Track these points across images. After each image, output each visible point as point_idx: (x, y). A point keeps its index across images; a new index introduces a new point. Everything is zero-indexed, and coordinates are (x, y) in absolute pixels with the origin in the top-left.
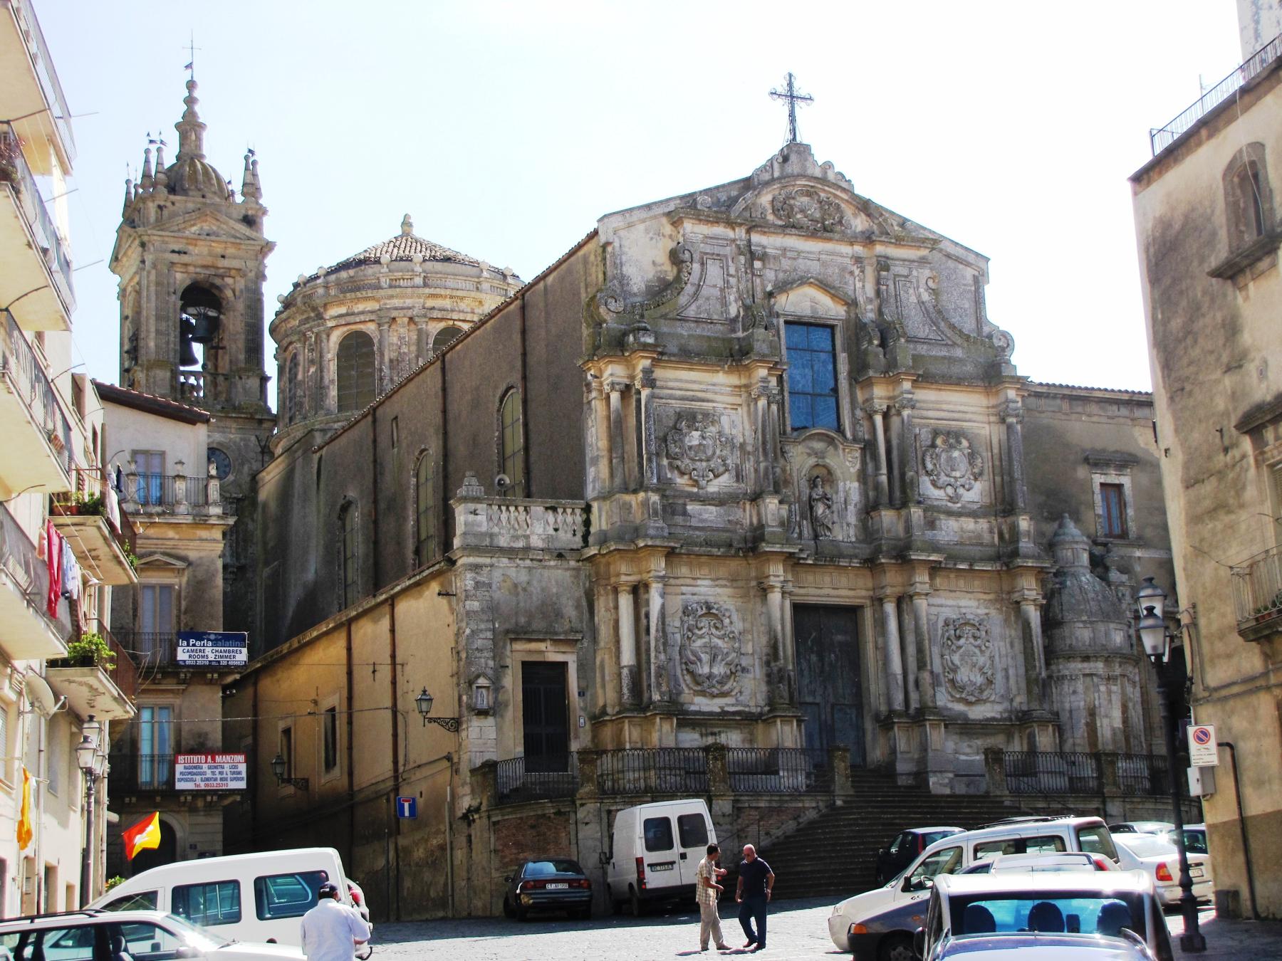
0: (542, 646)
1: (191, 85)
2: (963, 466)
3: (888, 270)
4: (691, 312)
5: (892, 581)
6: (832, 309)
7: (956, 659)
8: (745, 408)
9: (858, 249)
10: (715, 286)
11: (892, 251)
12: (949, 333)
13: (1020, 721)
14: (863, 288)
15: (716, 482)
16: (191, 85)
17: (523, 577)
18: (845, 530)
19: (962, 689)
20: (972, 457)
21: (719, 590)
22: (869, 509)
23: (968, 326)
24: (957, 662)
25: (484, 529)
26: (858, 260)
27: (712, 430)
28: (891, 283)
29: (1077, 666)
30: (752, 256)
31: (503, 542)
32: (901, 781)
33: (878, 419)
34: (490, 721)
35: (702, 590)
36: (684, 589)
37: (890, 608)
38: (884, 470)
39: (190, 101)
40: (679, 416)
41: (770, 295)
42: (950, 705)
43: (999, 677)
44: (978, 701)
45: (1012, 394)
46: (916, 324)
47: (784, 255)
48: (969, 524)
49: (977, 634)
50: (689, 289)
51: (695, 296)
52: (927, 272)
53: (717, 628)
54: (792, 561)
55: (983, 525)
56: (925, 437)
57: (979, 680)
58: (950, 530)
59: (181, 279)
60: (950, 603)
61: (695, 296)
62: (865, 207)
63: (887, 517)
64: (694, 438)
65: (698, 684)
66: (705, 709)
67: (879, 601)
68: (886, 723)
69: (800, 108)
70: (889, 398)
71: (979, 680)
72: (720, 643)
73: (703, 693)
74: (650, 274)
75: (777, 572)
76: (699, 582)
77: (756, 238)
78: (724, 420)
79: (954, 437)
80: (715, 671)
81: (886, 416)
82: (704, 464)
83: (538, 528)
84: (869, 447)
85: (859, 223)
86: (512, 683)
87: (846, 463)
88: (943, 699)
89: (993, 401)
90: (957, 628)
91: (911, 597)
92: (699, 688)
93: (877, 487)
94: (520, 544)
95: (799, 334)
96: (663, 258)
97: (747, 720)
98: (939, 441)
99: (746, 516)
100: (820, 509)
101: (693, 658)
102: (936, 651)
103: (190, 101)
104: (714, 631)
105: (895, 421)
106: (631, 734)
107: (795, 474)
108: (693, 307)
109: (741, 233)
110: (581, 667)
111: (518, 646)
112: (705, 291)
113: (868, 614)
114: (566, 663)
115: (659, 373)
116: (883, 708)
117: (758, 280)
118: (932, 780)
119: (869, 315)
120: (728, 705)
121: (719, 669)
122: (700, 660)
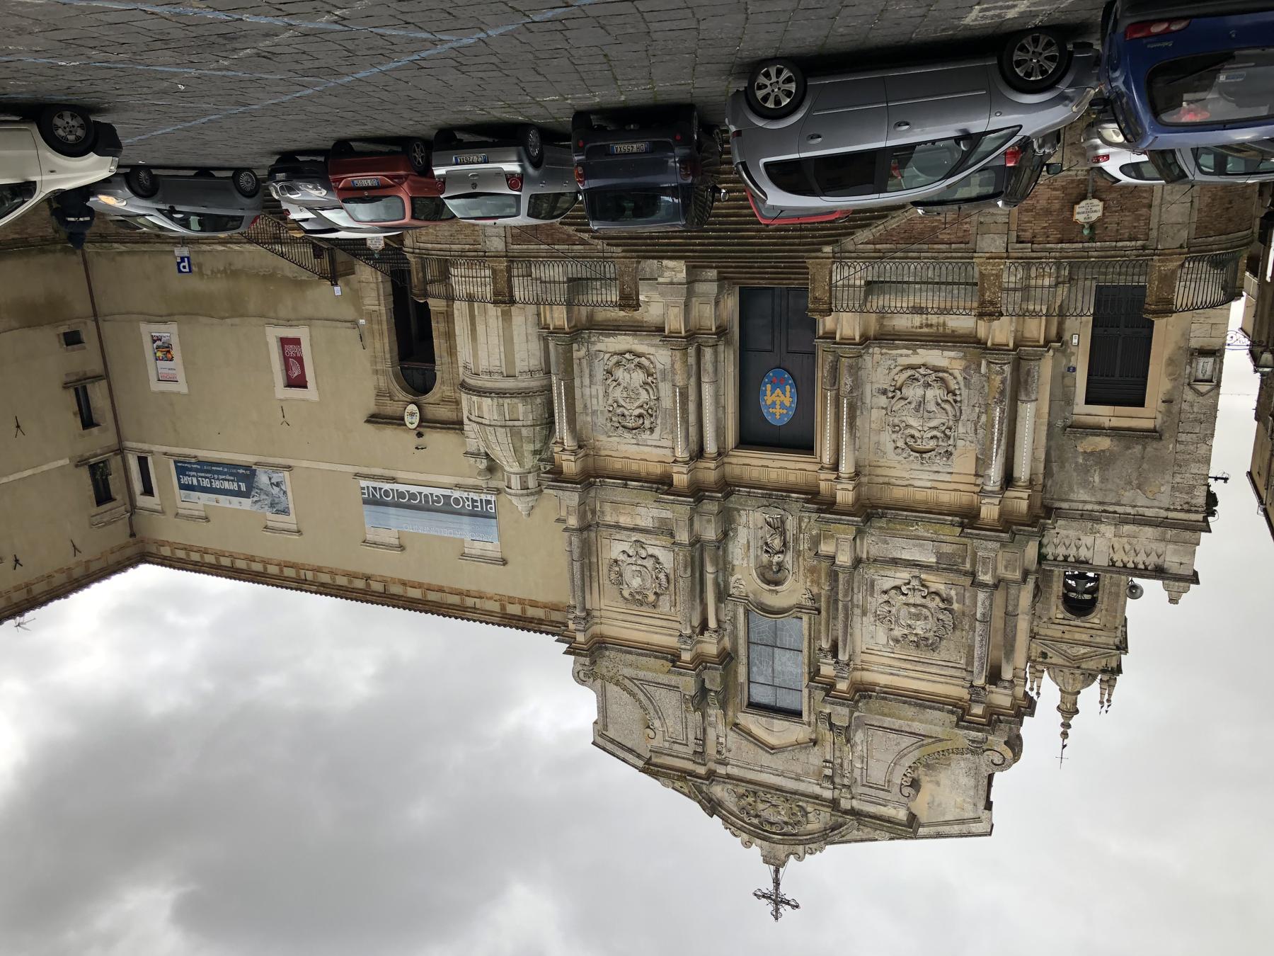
0: (1116, 423)
1: (1065, 735)
2: (627, 575)
3: (695, 752)
4: (907, 741)
5: (709, 472)
6: (750, 721)
7: (644, 396)
8: (858, 650)
9: (721, 770)
10: (878, 760)
11: (689, 766)
12: (636, 690)
13: (579, 331)
14: (718, 731)
15: (898, 582)
16: (1065, 735)
17: (1128, 496)
18: (751, 523)
19: (640, 366)
20: (620, 581)
21: (905, 474)
22: (726, 535)
23: (612, 689)
24: (643, 393)
25: (1171, 547)
26: (723, 763)
27: (898, 632)
28: (691, 737)
29: (524, 383)
30: (830, 778)
31: (1149, 531)
32: (713, 274)
33: (712, 624)
34: (1194, 344)
35: (925, 476)
36: (948, 478)
37: (711, 447)
38: (709, 578)
39: (1066, 725)
40: (933, 648)
41: (815, 742)
42: (652, 350)
43: (600, 374)
44: (622, 354)
45: (580, 637)
46: (669, 702)
47: (797, 774)
48: (624, 520)
49: (620, 419)
50: (907, 762)
51: (901, 755)
52: (655, 743)
53: (913, 437)
54: (824, 505)
55: (609, 518)
56: (665, 604)
57: (620, 373)
58: (648, 513)
59: (1095, 619)
60: (655, 450)
61: (901, 755)
62: (712, 807)
63: (710, 533)
64: (920, 628)
65: (942, 379)
66: (937, 352)
67: (721, 453)
68: (722, 331)
69: (768, 887)
70: (699, 642)
71: (620, 373)
72: (912, 422)
73: (936, 370)
74: (944, 777)
75: (845, 495)
76: (929, 484)
77: (828, 794)
78: (882, 637)
79: (638, 599)
80: (920, 392)
81: (704, 626)
82: (912, 601)
83: (1101, 544)
84: (723, 595)
85: (718, 791)
86: (1158, 383)
87: (745, 579)
88: (662, 357)
89: (597, 629)
90: (640, 425)
91: (691, 459)
92: (941, 374)
93: (715, 562)
94: (1127, 528)
95: (786, 701)
96: (927, 788)
97: (886, 338)
98: (652, 598)
99: (872, 546)
100: (777, 543)
101: (947, 406)
102: (667, 403)
103: (1066, 725)
104: (917, 434)
105: (696, 622)
106: (1035, 329)
107: (802, 577)
108: (904, 746)
109: (845, 804)
110: (1069, 401)
111: (1148, 424)
112: (890, 757)
113: (731, 438)
114: (1087, 402)
115: (964, 694)
116: (721, 348)
117: (828, 758)
118: (682, 276)
119: (714, 712)
120: (907, 356)
121: (914, 392)
122: (938, 404)
